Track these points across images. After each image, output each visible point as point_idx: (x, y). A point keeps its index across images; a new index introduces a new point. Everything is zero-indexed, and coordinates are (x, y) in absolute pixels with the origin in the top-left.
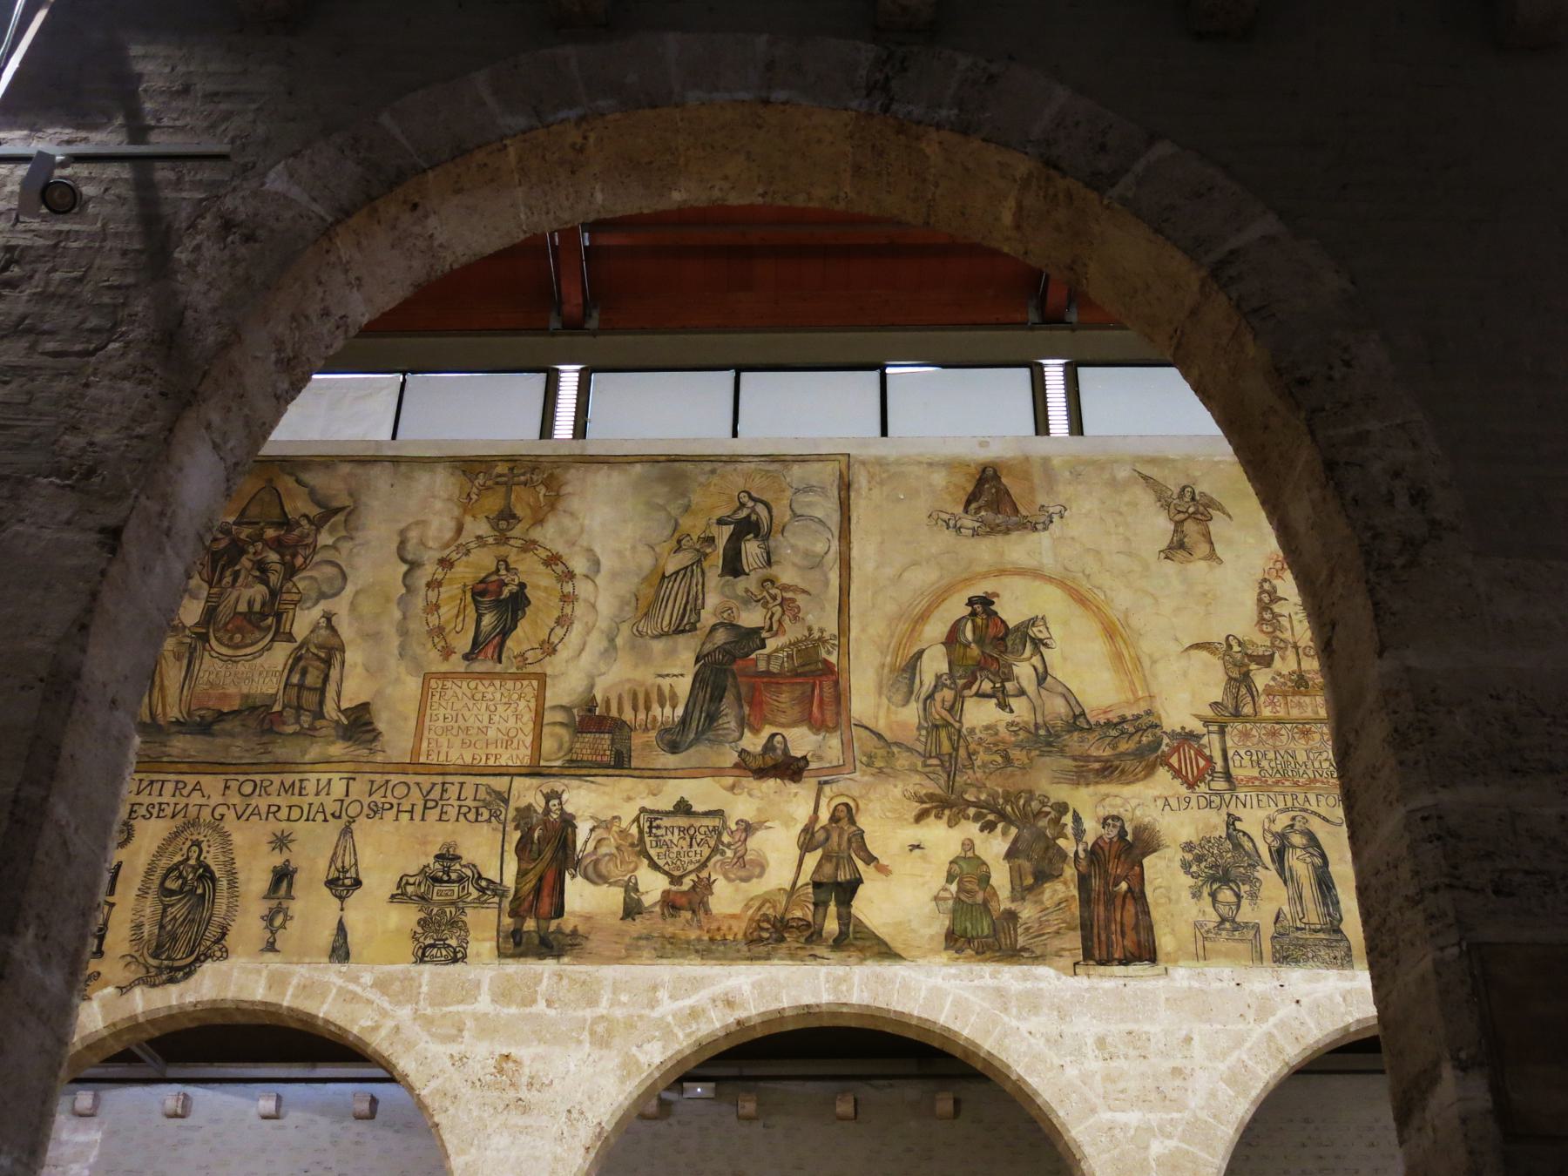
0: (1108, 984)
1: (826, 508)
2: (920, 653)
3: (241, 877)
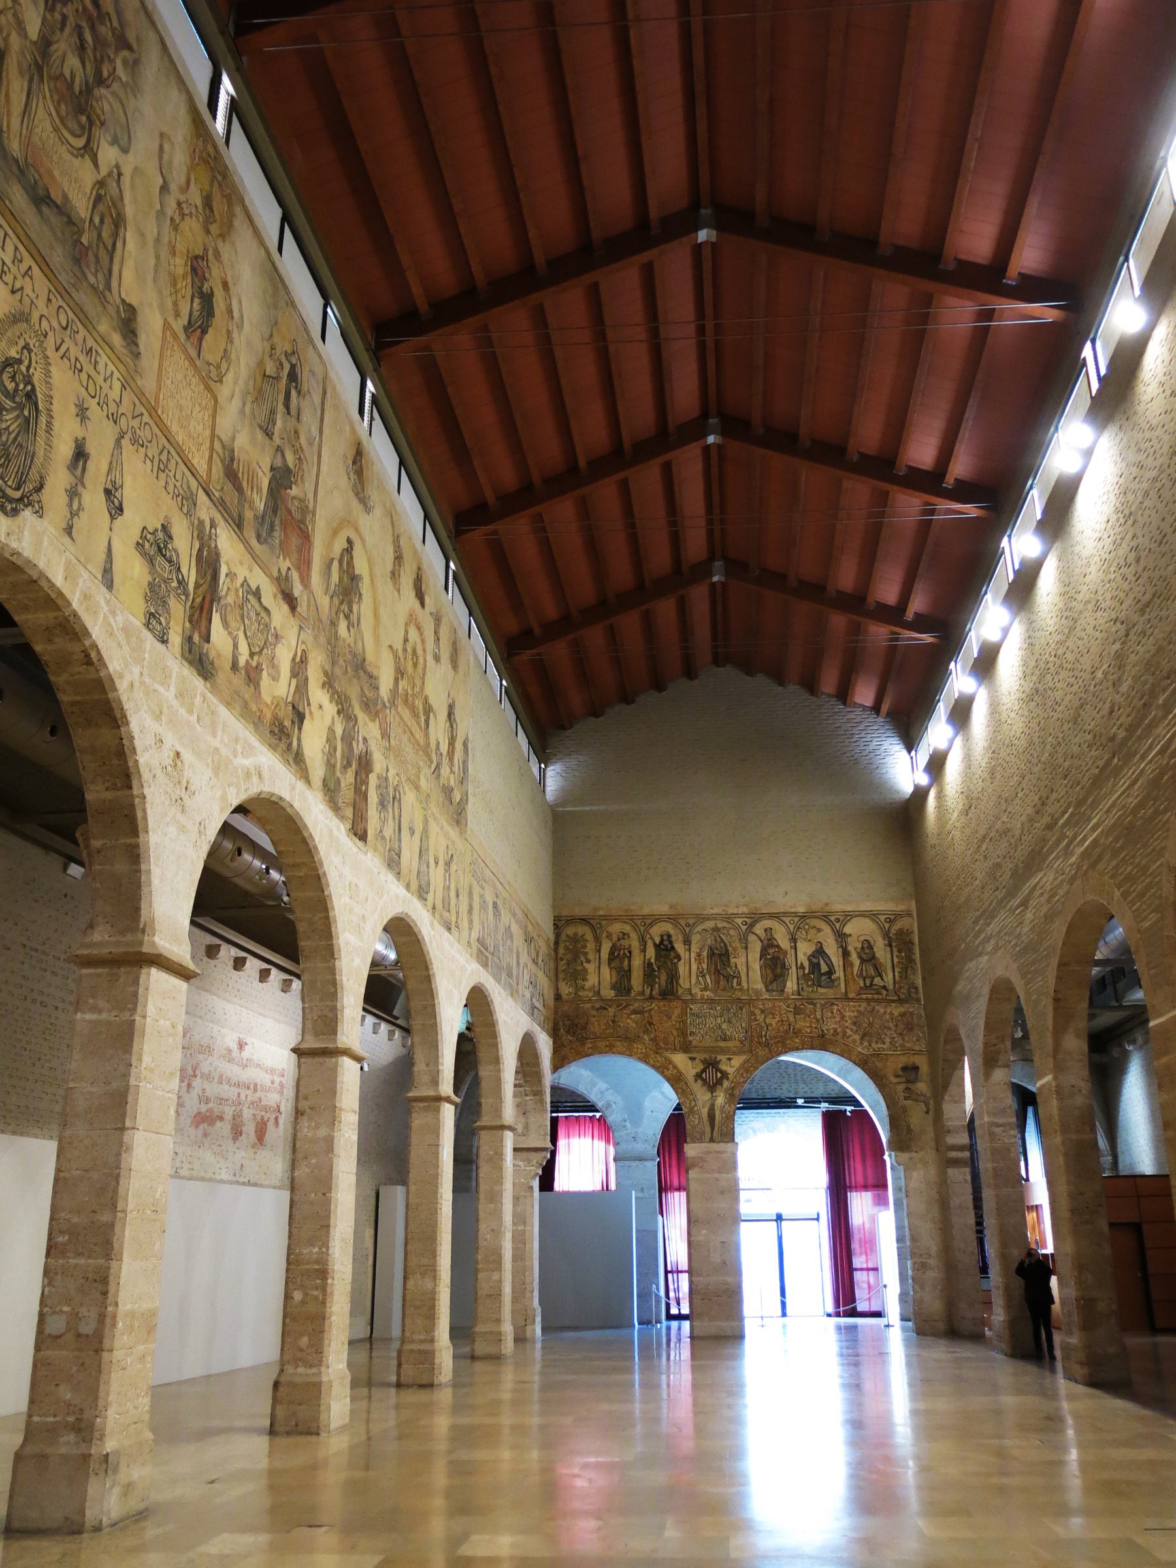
0: (355, 849)
1: (317, 400)
2: (332, 560)
3: (56, 425)
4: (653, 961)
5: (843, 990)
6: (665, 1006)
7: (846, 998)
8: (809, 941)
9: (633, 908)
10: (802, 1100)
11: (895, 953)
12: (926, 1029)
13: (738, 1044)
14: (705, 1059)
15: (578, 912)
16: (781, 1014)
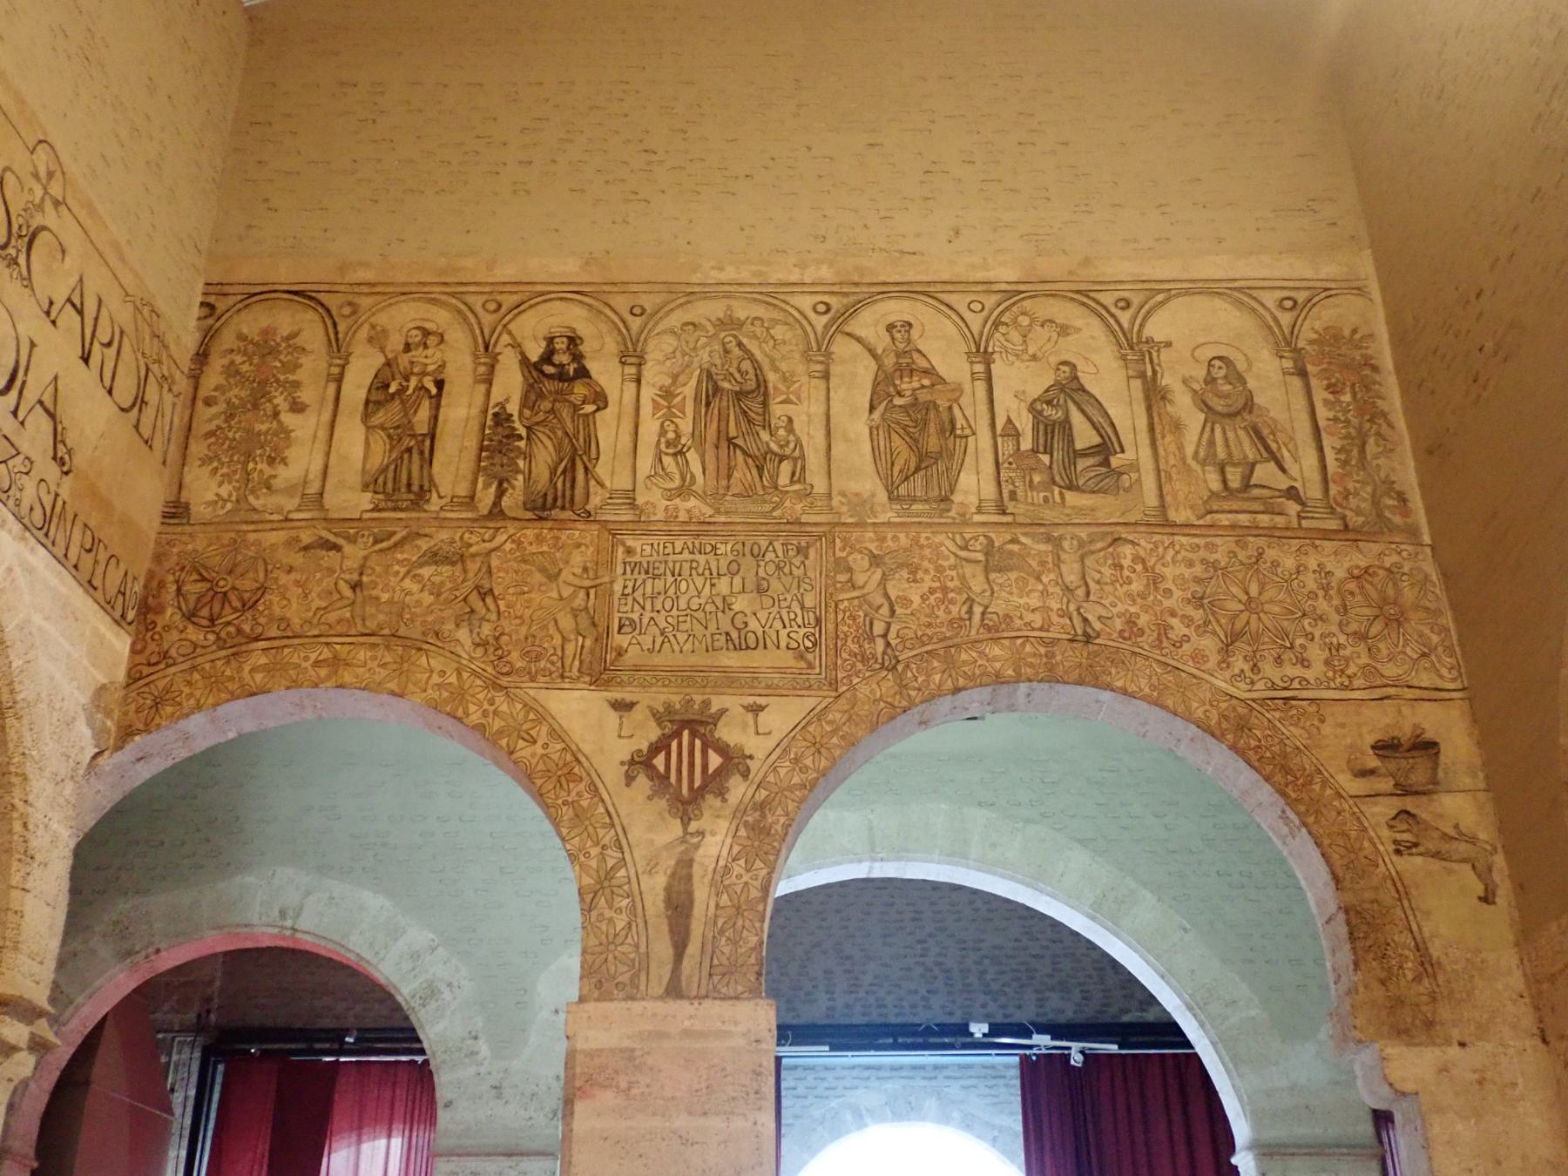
4: (513, 408)
5: (1152, 500)
6: (539, 539)
7: (1163, 522)
8: (1034, 358)
9: (469, 262)
10: (985, 1028)
11: (1320, 395)
12: (1448, 620)
13: (787, 659)
14: (669, 708)
15: (285, 274)
16: (940, 569)
